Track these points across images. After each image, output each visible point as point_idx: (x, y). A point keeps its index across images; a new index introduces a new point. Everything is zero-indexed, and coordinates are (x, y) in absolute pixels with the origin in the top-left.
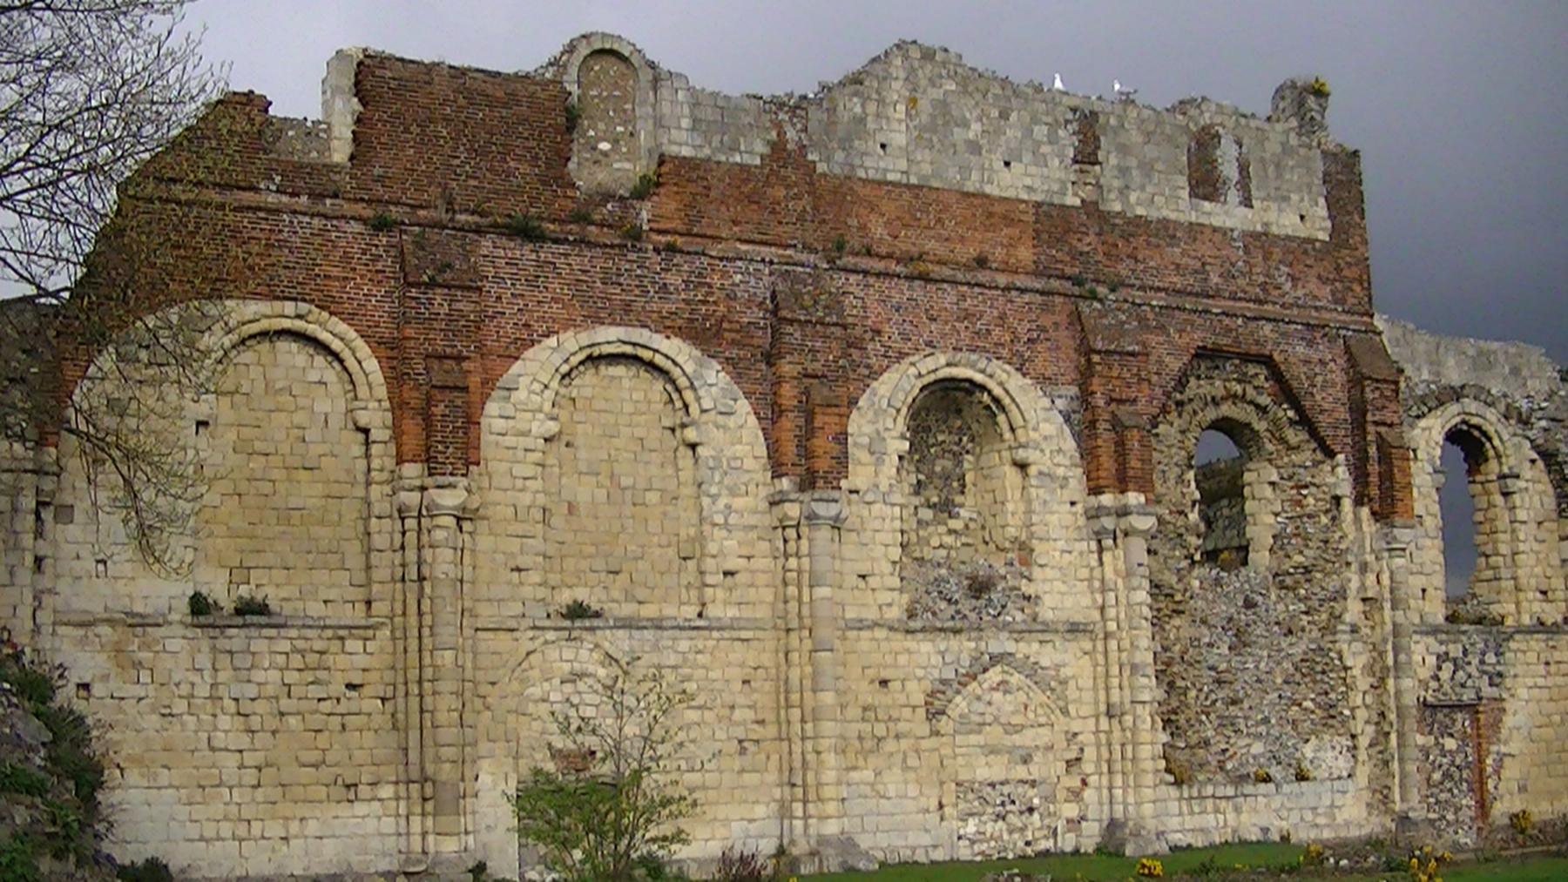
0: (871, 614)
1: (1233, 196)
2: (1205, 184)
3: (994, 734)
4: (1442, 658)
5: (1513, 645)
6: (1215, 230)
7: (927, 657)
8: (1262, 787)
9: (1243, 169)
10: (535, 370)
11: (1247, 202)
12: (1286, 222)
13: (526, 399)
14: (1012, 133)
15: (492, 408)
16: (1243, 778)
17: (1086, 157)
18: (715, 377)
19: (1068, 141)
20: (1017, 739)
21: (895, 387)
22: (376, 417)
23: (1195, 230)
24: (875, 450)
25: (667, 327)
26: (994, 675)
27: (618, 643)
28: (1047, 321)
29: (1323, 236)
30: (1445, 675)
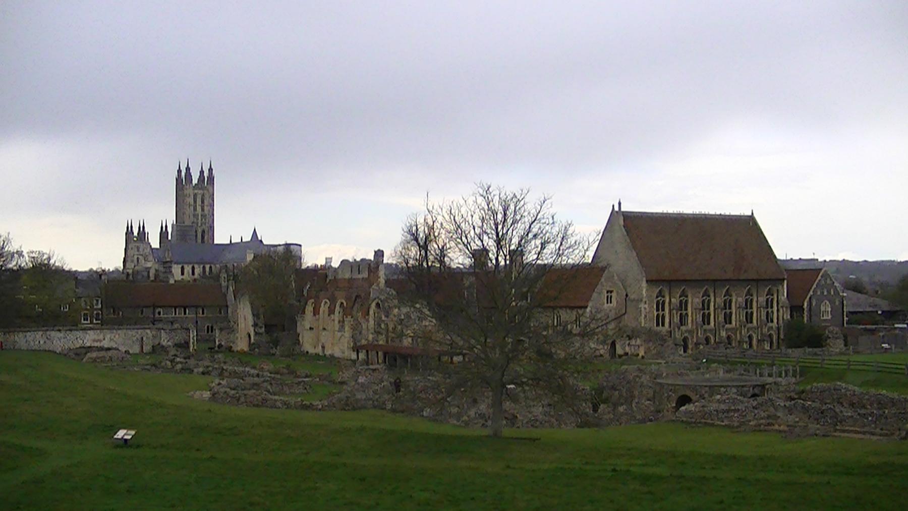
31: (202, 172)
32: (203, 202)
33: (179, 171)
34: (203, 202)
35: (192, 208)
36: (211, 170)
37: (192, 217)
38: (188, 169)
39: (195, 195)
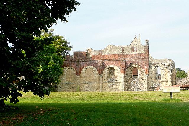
1: (135, 51)
2: (133, 51)
3: (114, 89)
7: (109, 84)
9: (136, 49)
10: (84, 69)
11: (137, 51)
12: (140, 53)
13: (83, 71)
14: (117, 50)
17: (123, 50)
18: (95, 68)
19: (121, 49)
22: (75, 72)
23: (132, 54)
24: (106, 72)
26: (114, 85)
28: (118, 62)
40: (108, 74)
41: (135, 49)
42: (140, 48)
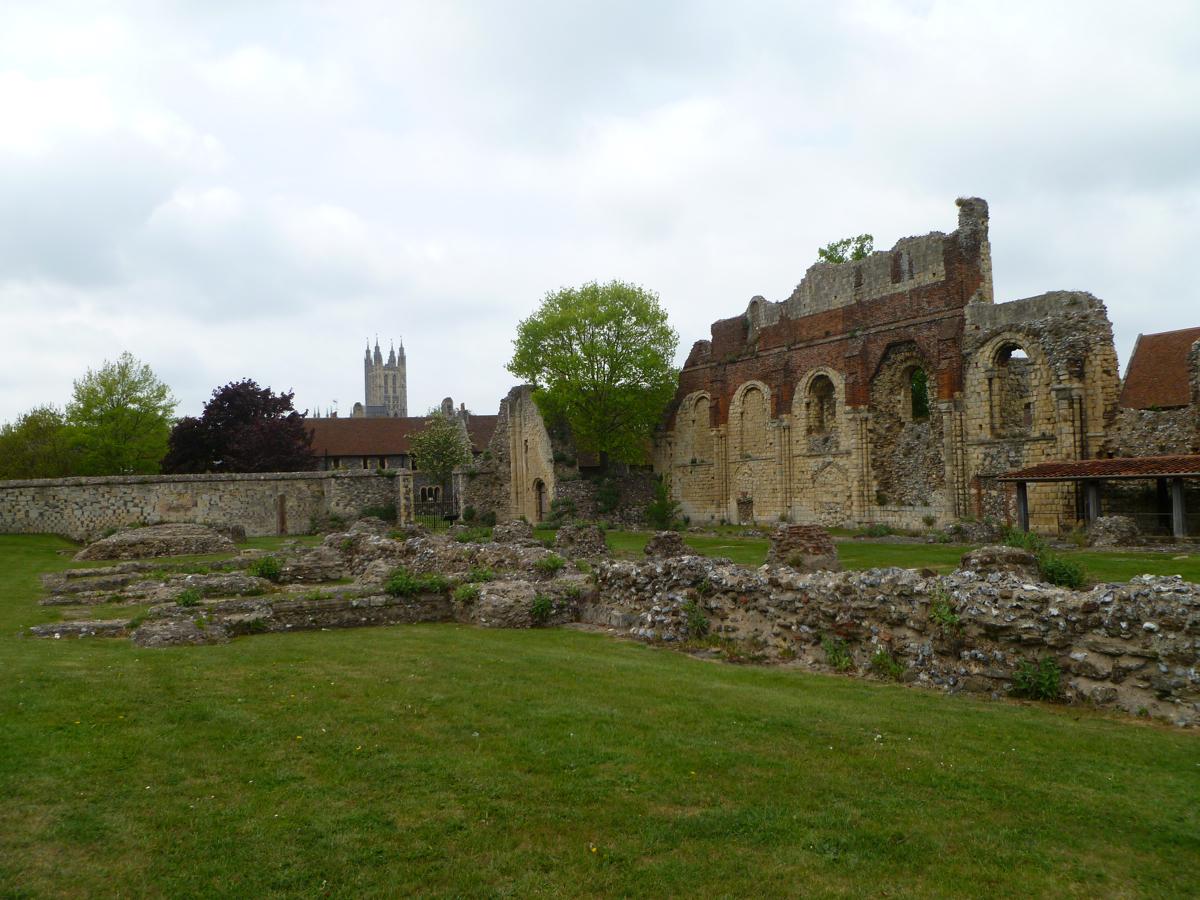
0: (798, 452)
4: (987, 455)
5: (1026, 447)
6: (899, 294)
7: (813, 464)
8: (908, 508)
9: (910, 264)
10: (737, 396)
11: (912, 277)
12: (927, 279)
15: (731, 407)
16: (903, 504)
19: (852, 279)
20: (833, 489)
21: (803, 384)
23: (892, 297)
25: (759, 379)
26: (828, 469)
27: (751, 464)
29: (943, 279)
30: (987, 463)
31: (392, 353)
32: (394, 383)
33: (368, 352)
34: (394, 383)
35: (383, 390)
36: (402, 349)
37: (382, 399)
38: (377, 348)
39: (386, 376)
40: (813, 412)
41: (905, 267)
42: (924, 256)
